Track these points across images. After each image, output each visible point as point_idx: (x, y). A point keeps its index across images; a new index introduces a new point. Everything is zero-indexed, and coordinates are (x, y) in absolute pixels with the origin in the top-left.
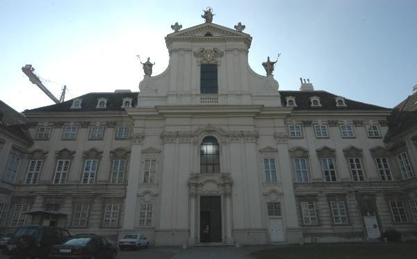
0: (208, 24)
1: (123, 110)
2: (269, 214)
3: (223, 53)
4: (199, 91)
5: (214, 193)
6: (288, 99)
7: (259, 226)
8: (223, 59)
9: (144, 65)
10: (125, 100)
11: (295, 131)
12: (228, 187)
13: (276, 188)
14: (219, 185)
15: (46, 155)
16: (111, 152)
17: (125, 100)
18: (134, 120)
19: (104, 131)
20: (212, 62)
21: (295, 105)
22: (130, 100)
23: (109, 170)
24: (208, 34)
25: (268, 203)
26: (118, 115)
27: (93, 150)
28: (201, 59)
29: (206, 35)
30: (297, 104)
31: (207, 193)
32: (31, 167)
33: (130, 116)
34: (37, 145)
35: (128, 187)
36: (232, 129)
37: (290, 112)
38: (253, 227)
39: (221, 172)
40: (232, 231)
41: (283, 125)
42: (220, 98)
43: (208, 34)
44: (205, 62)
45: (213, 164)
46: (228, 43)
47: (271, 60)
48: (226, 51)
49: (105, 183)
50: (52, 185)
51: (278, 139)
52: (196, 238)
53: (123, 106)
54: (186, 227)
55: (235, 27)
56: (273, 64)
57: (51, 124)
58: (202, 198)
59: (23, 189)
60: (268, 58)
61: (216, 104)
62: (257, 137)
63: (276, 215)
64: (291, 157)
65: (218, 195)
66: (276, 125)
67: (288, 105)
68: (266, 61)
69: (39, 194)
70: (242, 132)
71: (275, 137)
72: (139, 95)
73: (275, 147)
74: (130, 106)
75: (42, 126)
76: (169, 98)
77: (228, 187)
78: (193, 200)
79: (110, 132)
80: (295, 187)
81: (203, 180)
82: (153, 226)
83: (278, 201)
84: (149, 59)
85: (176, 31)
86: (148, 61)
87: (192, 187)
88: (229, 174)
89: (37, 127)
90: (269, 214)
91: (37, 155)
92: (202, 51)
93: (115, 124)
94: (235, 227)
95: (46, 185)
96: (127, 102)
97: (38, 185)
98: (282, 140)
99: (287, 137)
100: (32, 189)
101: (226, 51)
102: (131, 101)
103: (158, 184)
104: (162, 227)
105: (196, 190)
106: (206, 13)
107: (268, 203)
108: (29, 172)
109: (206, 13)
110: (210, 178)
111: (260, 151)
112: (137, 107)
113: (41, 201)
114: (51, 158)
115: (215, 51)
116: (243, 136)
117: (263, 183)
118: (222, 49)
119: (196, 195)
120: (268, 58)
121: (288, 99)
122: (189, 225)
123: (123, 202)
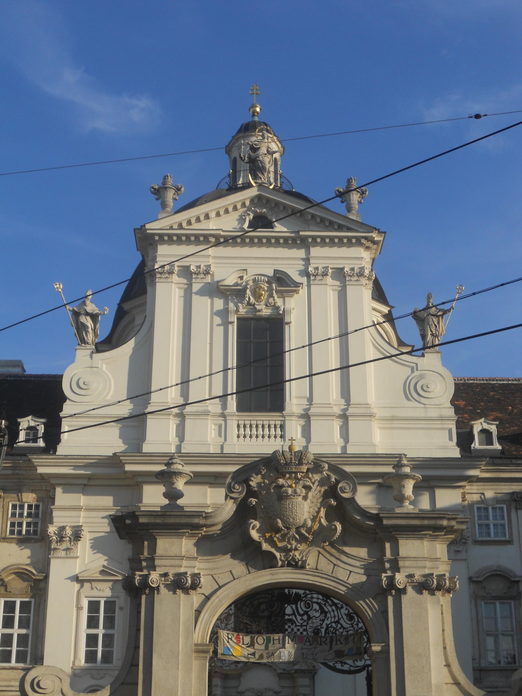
11: (491, 521)
30: (500, 443)
67: (476, 445)
76: (151, 422)
102: (41, 429)
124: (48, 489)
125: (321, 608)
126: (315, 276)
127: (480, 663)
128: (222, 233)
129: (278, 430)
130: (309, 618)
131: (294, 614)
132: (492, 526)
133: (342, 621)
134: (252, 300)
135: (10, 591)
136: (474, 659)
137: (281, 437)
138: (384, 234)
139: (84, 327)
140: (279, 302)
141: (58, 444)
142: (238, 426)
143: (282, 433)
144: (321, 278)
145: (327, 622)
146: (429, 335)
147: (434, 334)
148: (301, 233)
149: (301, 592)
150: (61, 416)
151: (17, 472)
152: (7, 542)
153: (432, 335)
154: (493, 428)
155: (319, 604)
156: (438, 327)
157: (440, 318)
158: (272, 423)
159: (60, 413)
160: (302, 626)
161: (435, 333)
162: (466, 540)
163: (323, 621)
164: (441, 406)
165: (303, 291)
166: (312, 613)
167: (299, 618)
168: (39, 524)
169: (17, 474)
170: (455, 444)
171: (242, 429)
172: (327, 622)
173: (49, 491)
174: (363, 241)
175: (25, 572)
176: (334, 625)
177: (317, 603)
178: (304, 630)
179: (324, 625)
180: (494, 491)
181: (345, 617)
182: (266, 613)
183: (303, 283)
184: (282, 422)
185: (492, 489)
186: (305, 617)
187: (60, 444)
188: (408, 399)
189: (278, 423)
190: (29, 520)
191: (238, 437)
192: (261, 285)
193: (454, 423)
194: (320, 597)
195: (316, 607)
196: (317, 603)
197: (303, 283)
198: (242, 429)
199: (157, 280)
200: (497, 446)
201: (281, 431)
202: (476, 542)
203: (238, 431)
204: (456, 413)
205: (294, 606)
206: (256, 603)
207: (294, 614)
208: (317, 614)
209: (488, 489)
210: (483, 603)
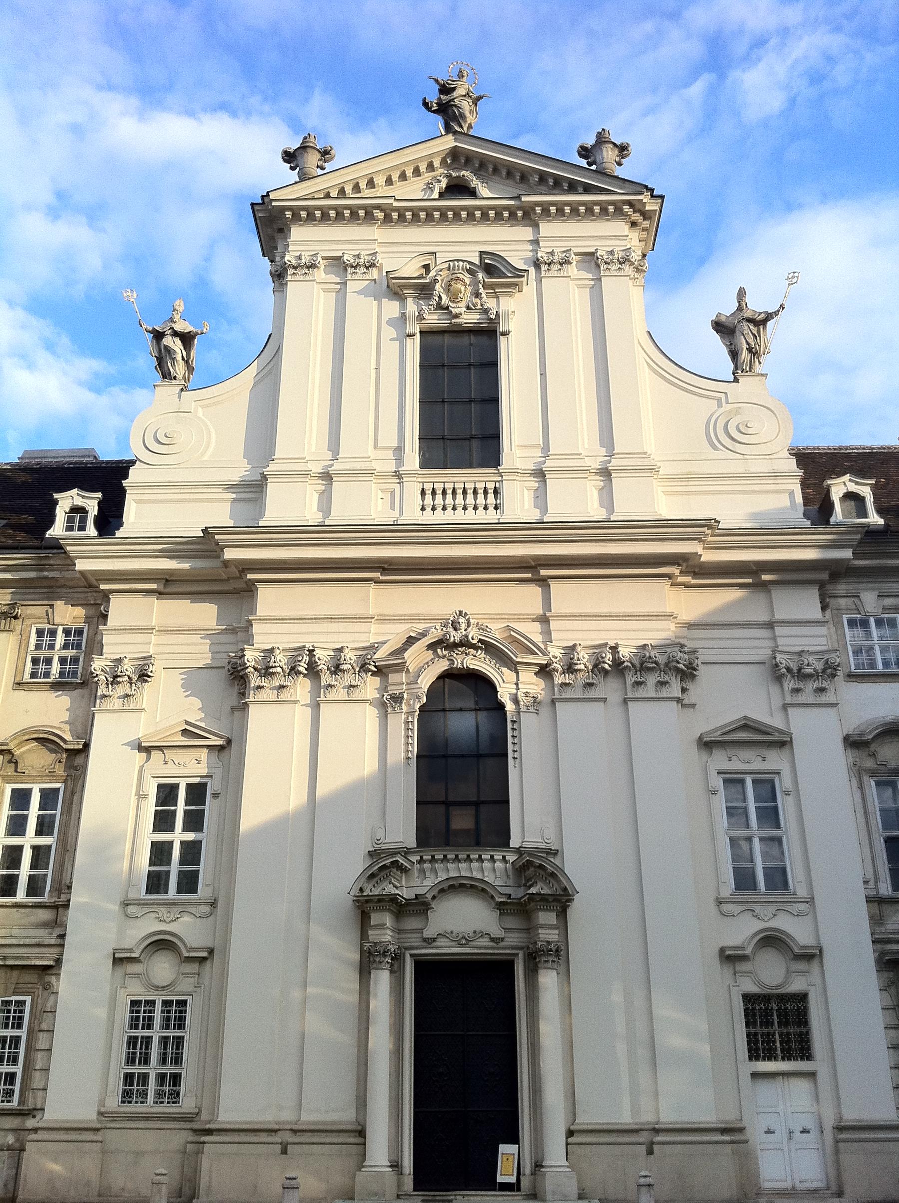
1: (56, 546)
2: (754, 1054)
3: (519, 273)
5: (481, 948)
6: (838, 487)
7: (707, 1116)
9: (158, 336)
10: (67, 500)
12: (547, 918)
13: (783, 923)
14: (504, 908)
17: (67, 500)
21: (875, 519)
22: (92, 503)
24: (457, 188)
25: (748, 998)
29: (441, 195)
30: (880, 511)
31: (446, 949)
35: (73, 916)
37: (847, 554)
38: (668, 1116)
39: (515, 842)
40: (570, 1133)
41: (815, 612)
42: (508, 488)
45: (477, 804)
46: (547, 228)
47: (756, 305)
51: (789, 684)
52: (396, 1165)
53: (58, 529)
54: (346, 1116)
55: (585, 152)
56: (760, 322)
58: (425, 968)
60: (741, 293)
61: (492, 516)
62: (688, 674)
63: (787, 1056)
64: (858, 772)
65: (501, 951)
66: (778, 616)
68: (728, 308)
71: (777, 674)
72: (135, 475)
73: (776, 721)
74: (92, 530)
76: (272, 488)
77: (547, 918)
78: (382, 980)
80: (876, 921)
81: (429, 882)
82: (187, 1103)
83: (796, 986)
87: (375, 918)
88: (555, 853)
90: (754, 1054)
94: (585, 1119)
96: (76, 509)
98: (811, 686)
99: (830, 671)
103: (213, 904)
104: (227, 1116)
105: (399, 931)
106: (445, 90)
107: (748, 998)
109: (445, 90)
110: (464, 870)
111: (707, 745)
112: (118, 534)
115: (490, 270)
117: (719, 902)
118: (517, 257)
119: (397, 958)
120: (741, 293)
121: (838, 487)
122: (361, 1102)
123: (47, 987)
124: (99, 602)
126: (549, 264)
127: (876, 888)
128: (395, 204)
129: (491, 496)
132: (877, 649)
134: (445, 301)
135: (24, 771)
136: (866, 882)
137: (496, 508)
138: (660, 201)
139: (169, 351)
140: (491, 303)
141: (119, 529)
142: (423, 492)
143: (498, 501)
144: (559, 267)
146: (745, 349)
147: (753, 348)
148: (524, 199)
150: (124, 485)
151: (46, 573)
152: (24, 690)
153: (750, 350)
154: (866, 492)
156: (758, 338)
157: (761, 327)
158: (481, 486)
159: (123, 481)
161: (753, 347)
162: (835, 670)
164: (775, 456)
165: (530, 288)
168: (81, 660)
169: (46, 578)
170: (802, 516)
171: (428, 497)
173: (100, 605)
174: (626, 208)
175: (51, 737)
180: (877, 593)
183: (528, 270)
184: (497, 483)
185: (873, 589)
187: (122, 529)
188: (715, 448)
190: (65, 653)
191: (423, 509)
192: (459, 275)
193: (798, 481)
197: (528, 270)
198: (428, 497)
199: (289, 277)
200: (875, 519)
201: (496, 499)
202: (851, 677)
203: (423, 500)
204: (798, 464)
209: (866, 589)
210: (873, 783)
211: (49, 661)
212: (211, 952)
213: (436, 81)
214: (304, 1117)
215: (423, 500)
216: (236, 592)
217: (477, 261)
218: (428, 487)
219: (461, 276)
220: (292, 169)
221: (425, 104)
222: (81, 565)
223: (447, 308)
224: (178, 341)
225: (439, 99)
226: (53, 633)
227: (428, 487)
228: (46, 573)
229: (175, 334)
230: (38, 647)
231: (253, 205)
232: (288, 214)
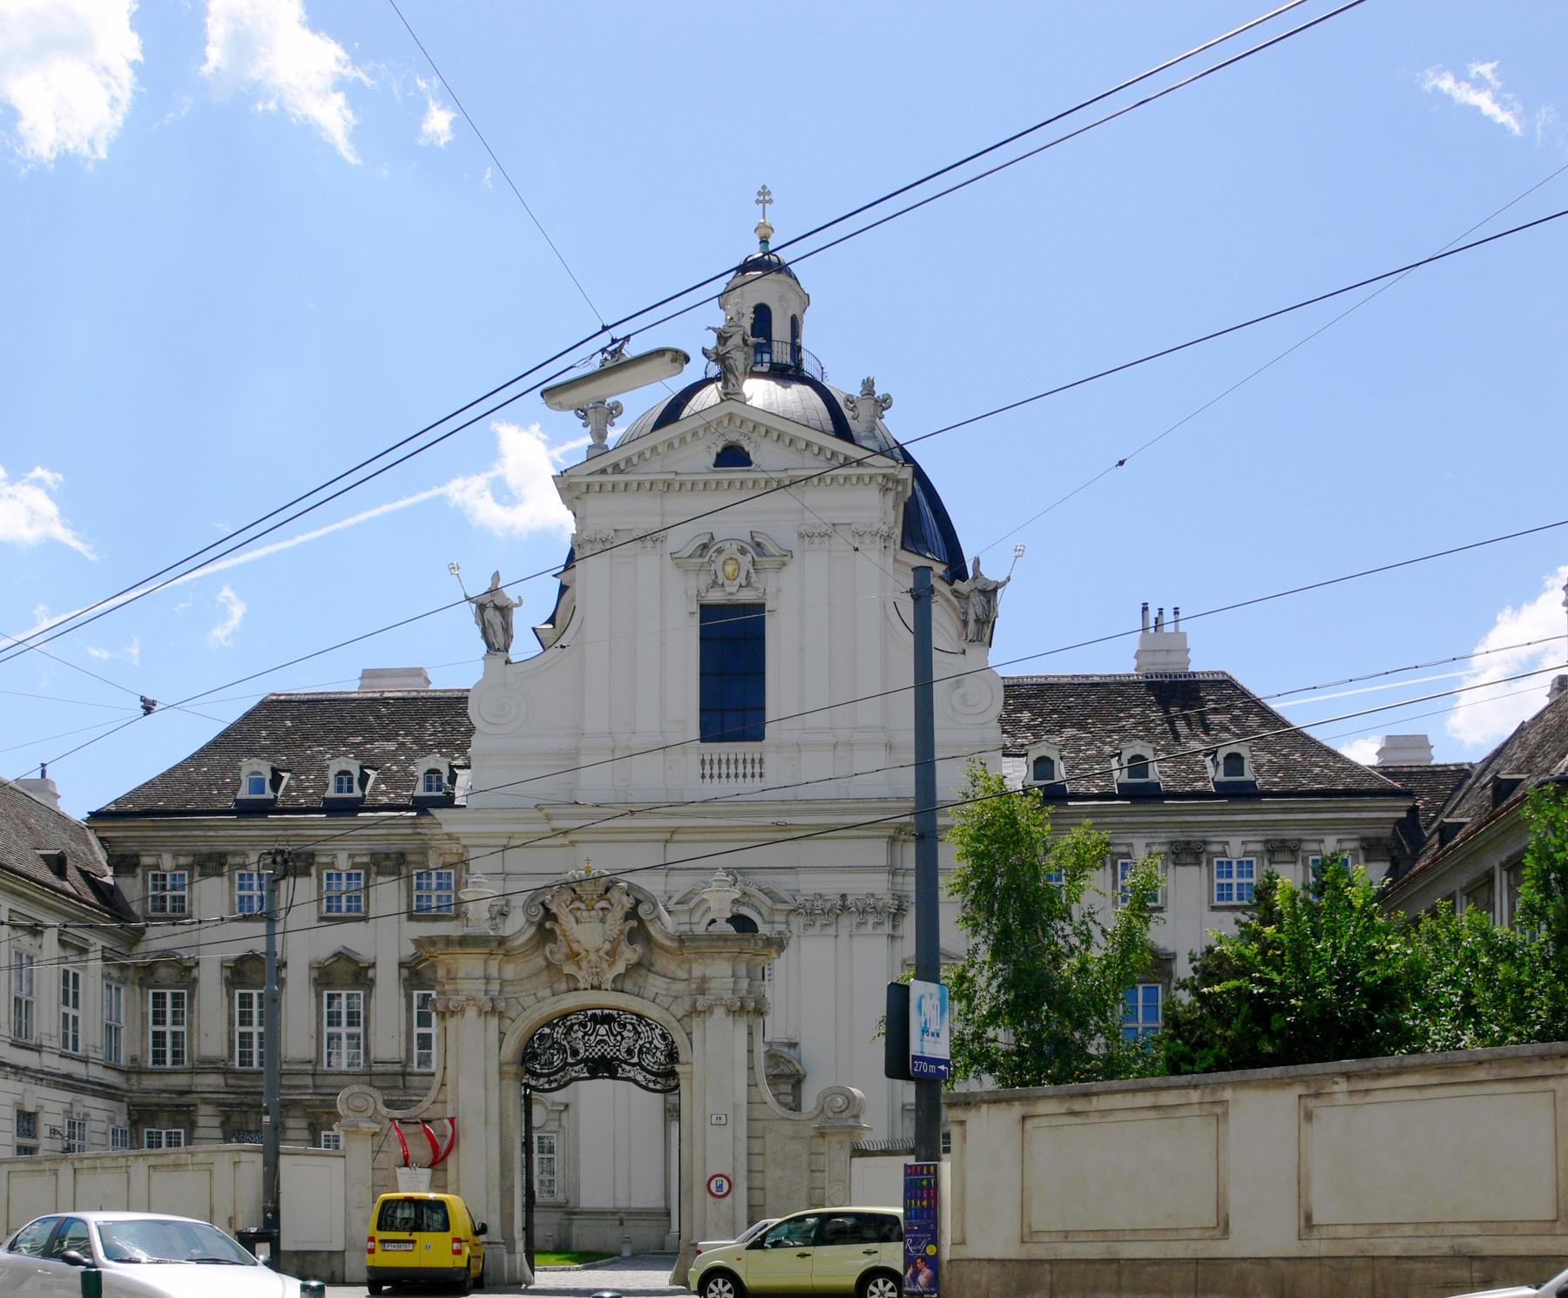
0: (732, 407)
4: (695, 732)
8: (789, 576)
9: (482, 608)
15: (195, 972)
16: (401, 965)
18: (465, 846)
19: (367, 887)
20: (746, 596)
23: (403, 1028)
24: (733, 456)
26: (409, 831)
27: (343, 956)
28: (705, 580)
32: (156, 1014)
33: (450, 836)
34: (159, 939)
36: (809, 885)
42: (771, 761)
43: (733, 456)
44: (716, 597)
48: (801, 536)
49: (397, 1068)
50: (234, 1072)
57: (182, 860)
59: (151, 1082)
69: (206, 1102)
70: (844, 897)
75: (157, 867)
79: (387, 894)
84: (496, 576)
85: (600, 435)
86: (493, 591)
89: (139, 871)
91: (163, 973)
92: (705, 547)
93: (401, 857)
95: (217, 1071)
97: (193, 1072)
100: (181, 1081)
101: (801, 536)
108: (152, 1028)
113: (216, 1122)
114: (210, 981)
116: (844, 908)
125: (635, 1028)
129: (757, 766)
130: (623, 1038)
131: (607, 1034)
133: (655, 1042)
145: (640, 1042)
149: (615, 1012)
153: (977, 621)
155: (633, 1024)
160: (615, 1046)
163: (637, 1041)
166: (625, 1034)
167: (612, 1038)
171: (707, 767)
172: (640, 1042)
176: (648, 1045)
177: (630, 1023)
178: (618, 1050)
179: (638, 1046)
181: (659, 1037)
182: (580, 1034)
186: (619, 1038)
189: (757, 757)
191: (703, 777)
194: (635, 1017)
195: (629, 1027)
196: (630, 1023)
198: (707, 767)
203: (703, 769)
205: (607, 1027)
206: (569, 1023)
207: (607, 1034)
208: (631, 1035)
211: (429, 897)
212: (567, 1106)
213: (714, 329)
214: (634, 1205)
215: (703, 769)
216: (563, 846)
217: (748, 539)
218: (707, 758)
219: (734, 556)
220: (585, 426)
221: (705, 352)
222: (446, 829)
223: (723, 585)
224: (497, 613)
225: (716, 348)
226: (429, 875)
227: (707, 758)
228: (419, 830)
229: (496, 607)
230: (419, 887)
231: (553, 477)
232: (584, 488)
